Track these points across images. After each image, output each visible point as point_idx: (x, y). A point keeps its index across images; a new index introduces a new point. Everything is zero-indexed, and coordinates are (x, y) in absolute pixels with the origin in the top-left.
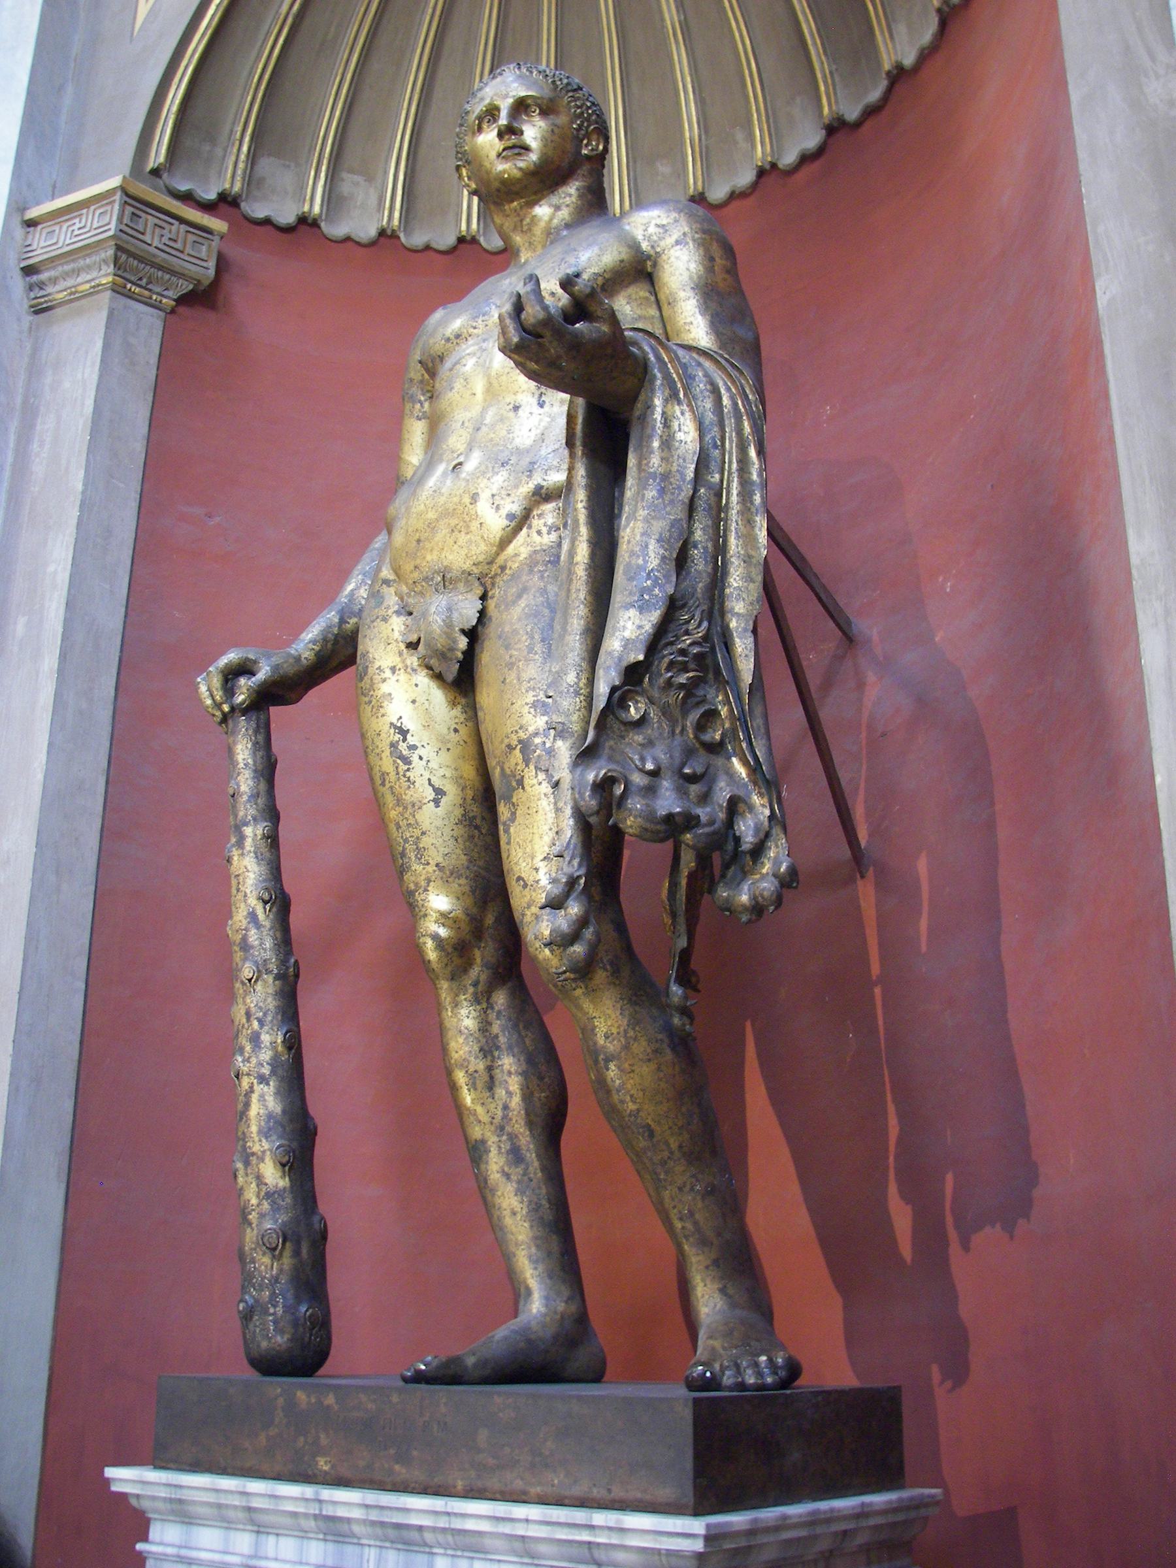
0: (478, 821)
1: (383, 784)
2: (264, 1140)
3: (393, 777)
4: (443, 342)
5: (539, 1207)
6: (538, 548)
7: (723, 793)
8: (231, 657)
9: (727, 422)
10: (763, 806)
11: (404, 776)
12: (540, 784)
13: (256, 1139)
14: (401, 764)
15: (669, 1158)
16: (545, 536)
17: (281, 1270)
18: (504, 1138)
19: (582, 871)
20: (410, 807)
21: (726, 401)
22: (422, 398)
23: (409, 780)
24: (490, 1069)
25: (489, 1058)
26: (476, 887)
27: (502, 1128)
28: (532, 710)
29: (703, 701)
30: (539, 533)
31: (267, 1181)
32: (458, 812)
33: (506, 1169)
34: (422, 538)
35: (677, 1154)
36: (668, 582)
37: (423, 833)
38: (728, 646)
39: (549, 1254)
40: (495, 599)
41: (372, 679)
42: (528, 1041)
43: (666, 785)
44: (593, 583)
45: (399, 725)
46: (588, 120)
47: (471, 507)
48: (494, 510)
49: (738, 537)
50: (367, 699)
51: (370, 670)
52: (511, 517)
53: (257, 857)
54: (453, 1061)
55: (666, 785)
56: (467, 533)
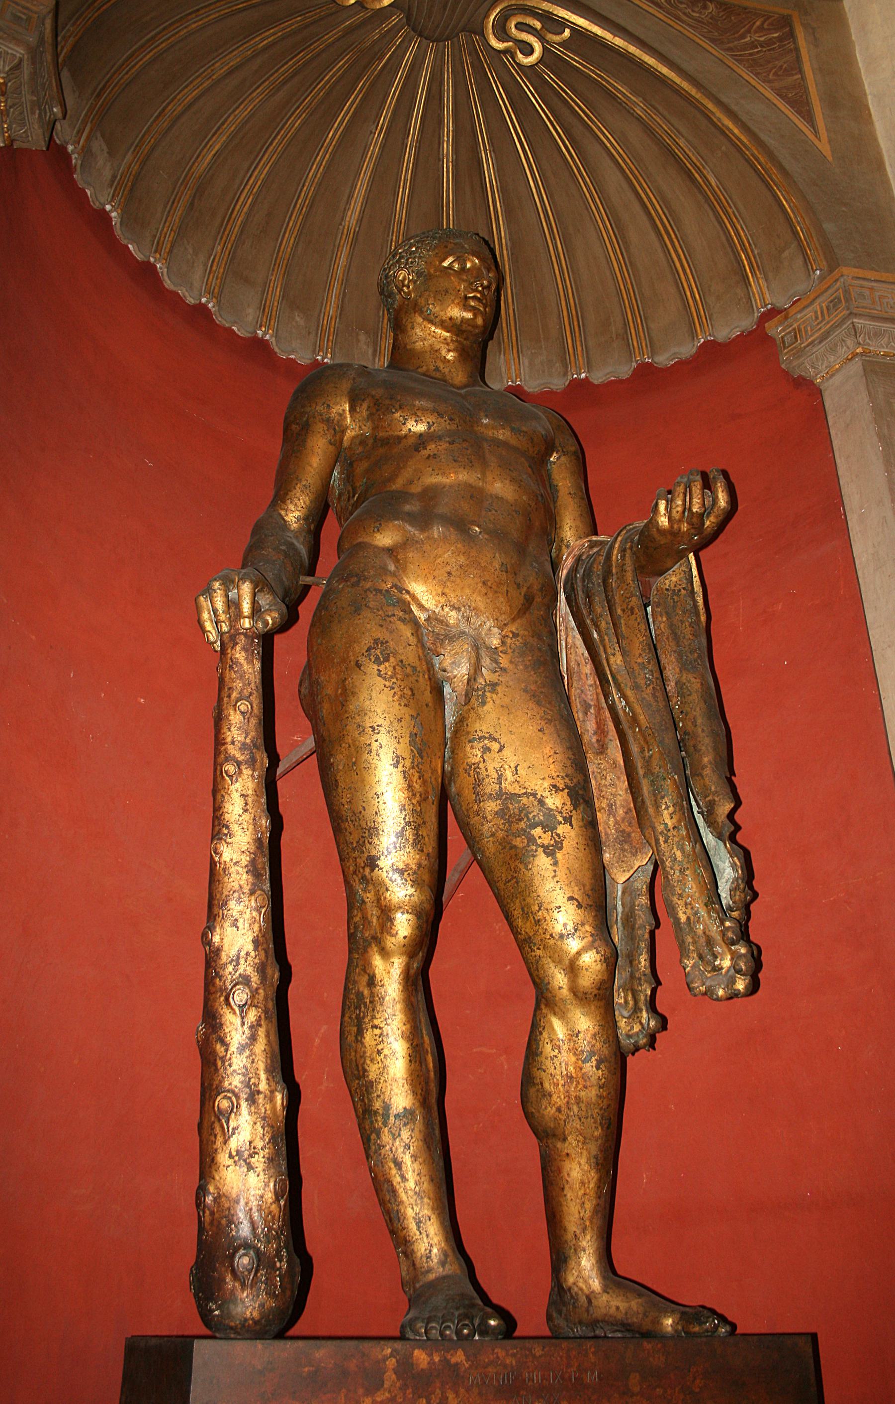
13: (263, 1076)
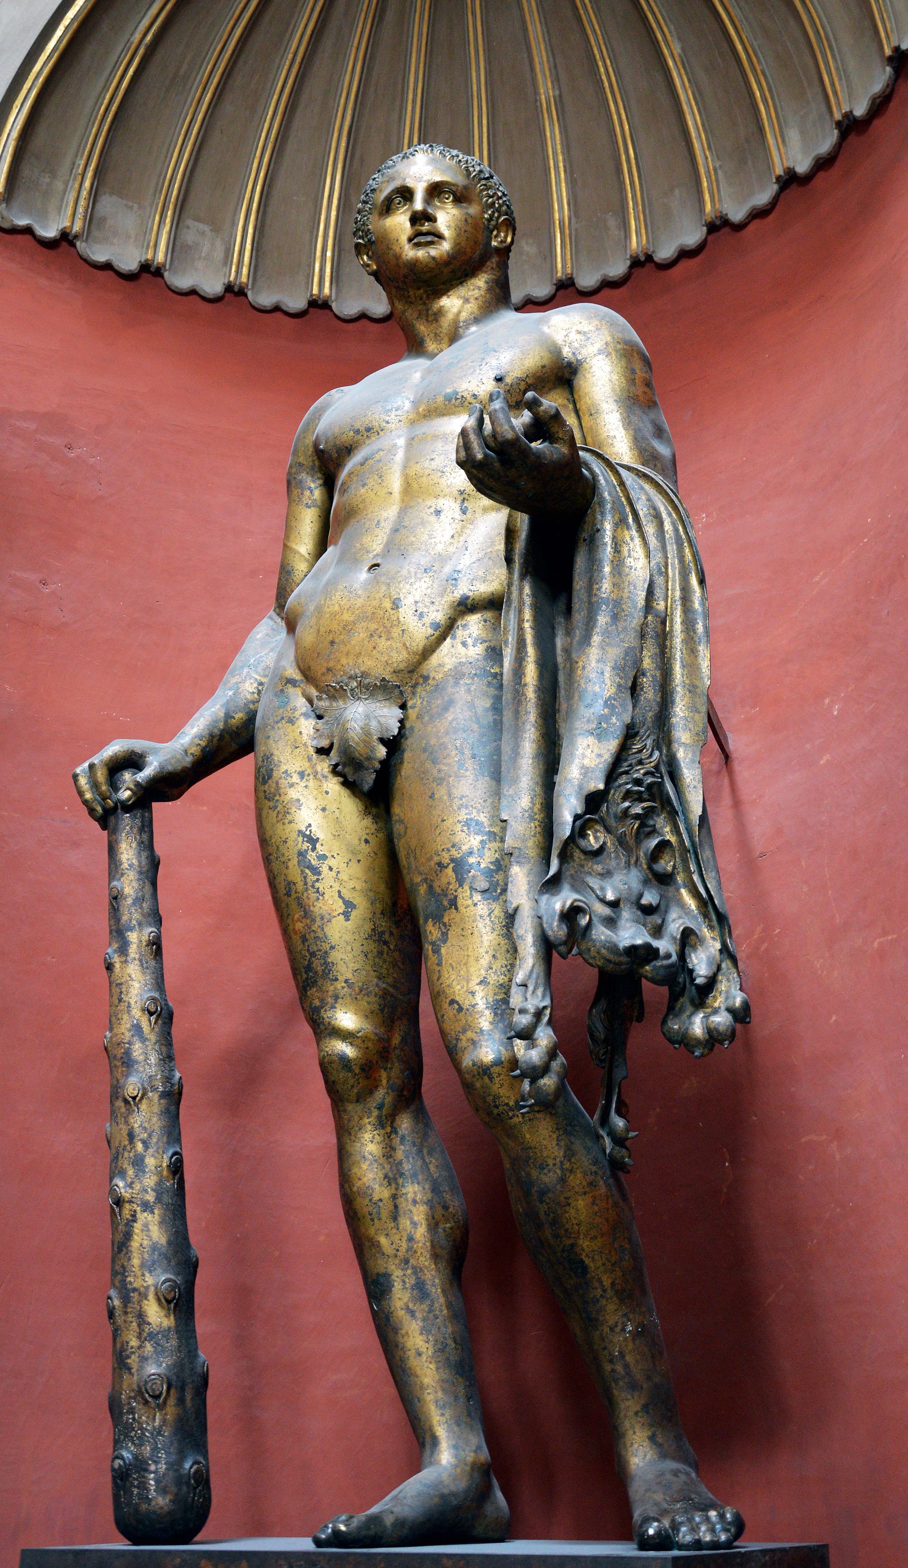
0: (386, 937)
1: (288, 894)
2: (147, 1275)
3: (300, 886)
4: (352, 433)
5: (445, 1347)
6: (464, 660)
7: (675, 925)
8: (114, 748)
9: (669, 548)
10: (713, 938)
11: (313, 886)
12: (475, 905)
14: (310, 874)
15: (601, 1296)
16: (471, 648)
17: (164, 1421)
18: (409, 1271)
19: (547, 1002)
20: (318, 919)
21: (668, 526)
22: (312, 485)
23: (318, 892)
24: (394, 1197)
25: (394, 1185)
26: (385, 1005)
27: (407, 1261)
28: (465, 828)
29: (654, 831)
30: (464, 644)
31: (150, 1320)
32: (368, 927)
33: (411, 1305)
34: (337, 641)
35: (610, 1293)
36: (625, 710)
37: (332, 948)
38: (674, 776)
39: (456, 1398)
40: (417, 709)
41: (277, 783)
42: (432, 1168)
43: (626, 914)
44: (542, 706)
45: (308, 833)
46: (499, 210)
47: (392, 612)
48: (416, 618)
49: (683, 667)
50: (271, 804)
51: (275, 774)
52: (436, 626)
53: (142, 965)
54: (355, 1189)
55: (626, 914)
56: (388, 639)
